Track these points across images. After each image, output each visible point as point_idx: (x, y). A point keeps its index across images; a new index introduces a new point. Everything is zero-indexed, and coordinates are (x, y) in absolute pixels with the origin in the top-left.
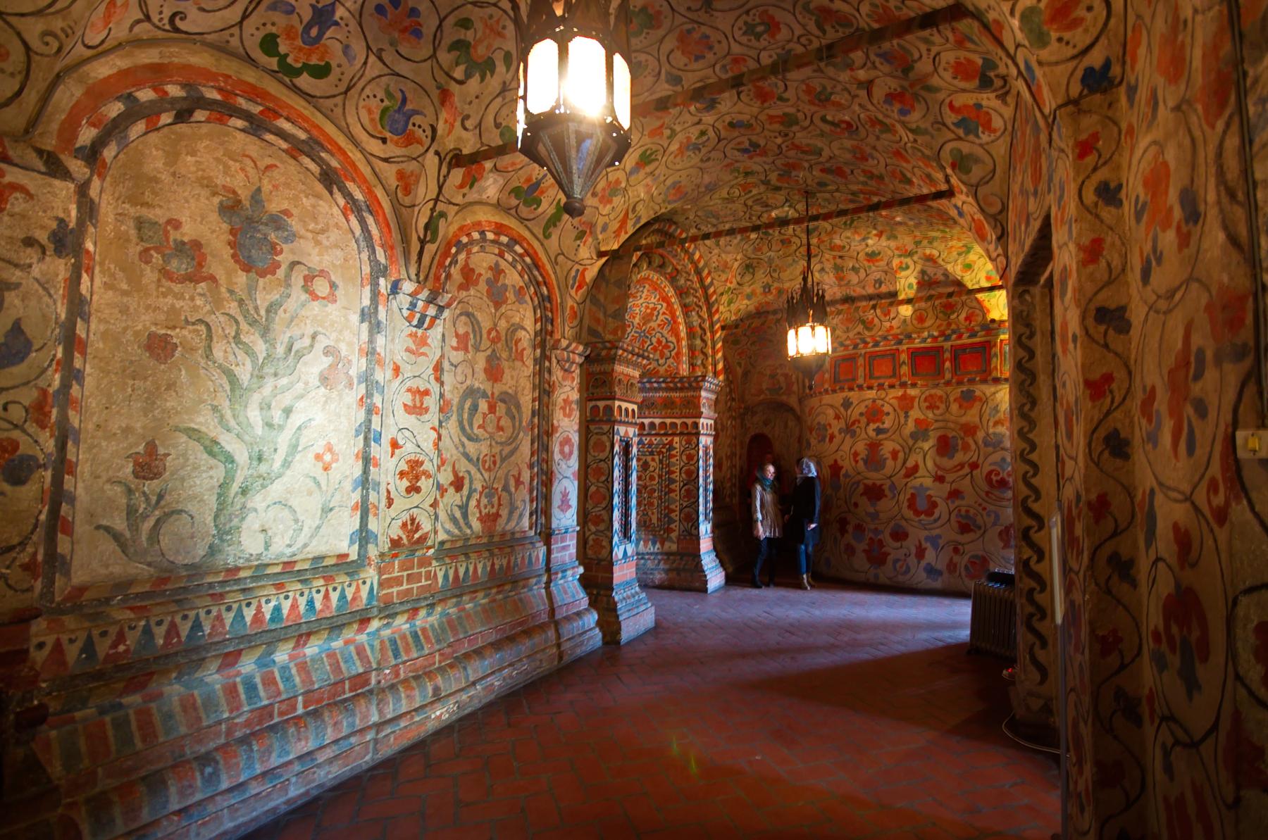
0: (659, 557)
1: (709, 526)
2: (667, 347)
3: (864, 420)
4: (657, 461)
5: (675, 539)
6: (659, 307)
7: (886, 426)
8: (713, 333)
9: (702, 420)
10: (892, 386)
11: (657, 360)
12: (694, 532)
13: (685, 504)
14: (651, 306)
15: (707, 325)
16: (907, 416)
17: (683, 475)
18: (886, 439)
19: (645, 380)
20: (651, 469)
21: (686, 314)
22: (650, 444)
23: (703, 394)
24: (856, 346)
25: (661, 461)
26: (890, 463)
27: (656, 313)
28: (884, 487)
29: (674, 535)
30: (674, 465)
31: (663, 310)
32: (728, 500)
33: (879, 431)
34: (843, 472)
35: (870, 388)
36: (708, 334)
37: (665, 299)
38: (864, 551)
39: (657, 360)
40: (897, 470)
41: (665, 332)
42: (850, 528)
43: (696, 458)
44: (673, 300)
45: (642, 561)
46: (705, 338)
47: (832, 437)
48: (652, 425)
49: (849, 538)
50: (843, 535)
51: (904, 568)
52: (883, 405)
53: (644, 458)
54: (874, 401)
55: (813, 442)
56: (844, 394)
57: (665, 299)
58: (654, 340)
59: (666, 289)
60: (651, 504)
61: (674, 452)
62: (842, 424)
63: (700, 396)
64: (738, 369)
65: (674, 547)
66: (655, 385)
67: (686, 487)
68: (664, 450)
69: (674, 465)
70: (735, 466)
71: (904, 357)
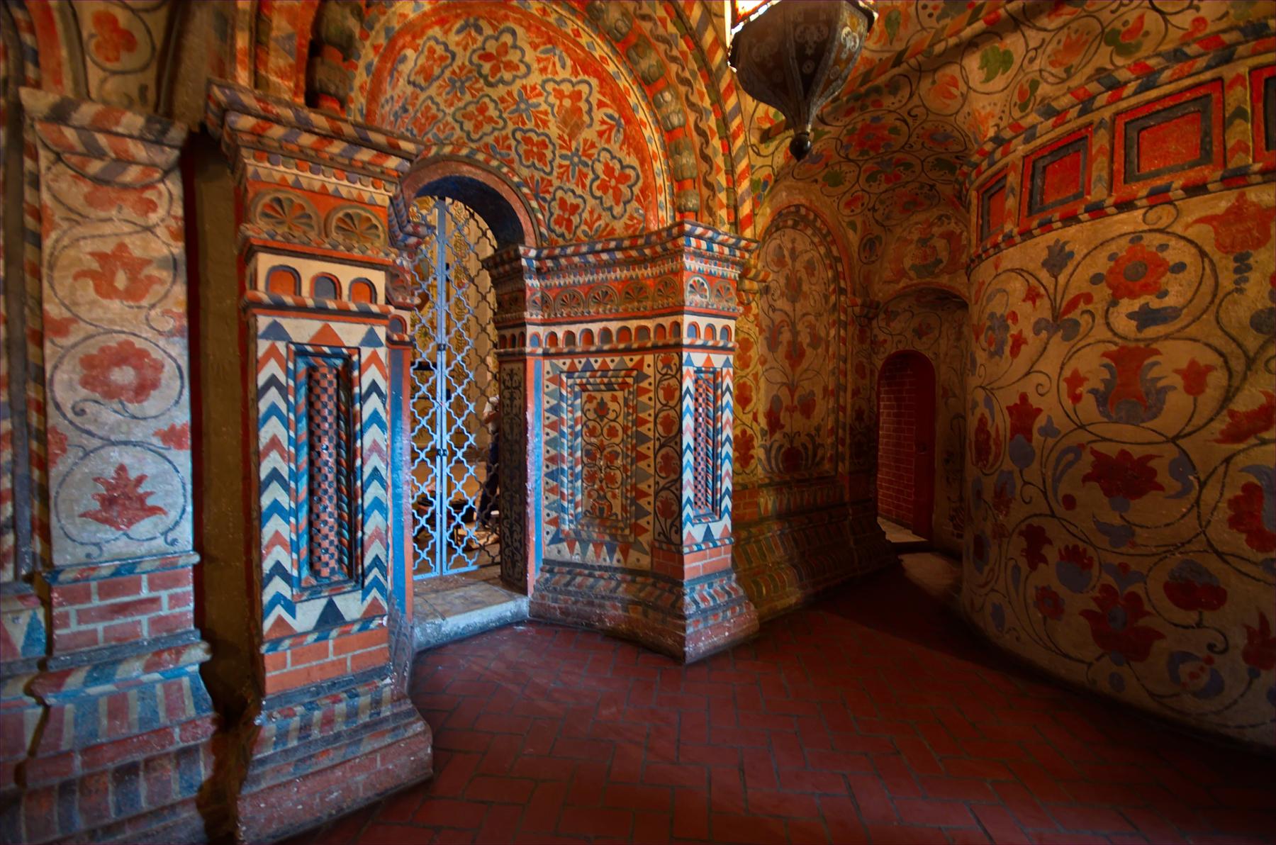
0: (619, 576)
1: (722, 526)
2: (624, 178)
3: (1102, 293)
4: (621, 402)
5: (647, 548)
6: (584, 89)
7: (1169, 301)
8: (727, 141)
9: (687, 320)
10: (1197, 189)
11: (610, 209)
12: (674, 538)
13: (662, 483)
14: (567, 88)
15: (712, 121)
16: (1243, 266)
17: (660, 428)
18: (1167, 337)
19: (584, 249)
20: (612, 415)
21: (654, 104)
22: (605, 370)
23: (690, 263)
24: (1086, 103)
25: (626, 400)
26: (1178, 401)
27: (584, 107)
28: (1152, 464)
29: (645, 539)
30: (645, 408)
31: (596, 97)
32: (827, 466)
33: (1145, 318)
34: (1040, 421)
35: (1125, 205)
36: (716, 142)
37: (588, 65)
38: (1087, 614)
39: (610, 209)
40: (1197, 421)
41: (614, 147)
42: (1051, 553)
43: (677, 394)
44: (611, 68)
45: (591, 580)
46: (709, 152)
47: (1018, 342)
48: (606, 333)
49: (1047, 575)
50: (1033, 567)
51: (1205, 679)
52: (1164, 247)
53: (598, 395)
54: (1136, 238)
55: (981, 357)
56: (1050, 238)
57: (588, 65)
58: (599, 168)
59: (584, 40)
60: (611, 479)
61: (645, 384)
62: (1043, 310)
63: (683, 268)
64: (851, 234)
65: (646, 561)
66: (605, 256)
67: (663, 451)
68: (630, 380)
69: (645, 408)
70: (843, 409)
71: (1240, 96)
